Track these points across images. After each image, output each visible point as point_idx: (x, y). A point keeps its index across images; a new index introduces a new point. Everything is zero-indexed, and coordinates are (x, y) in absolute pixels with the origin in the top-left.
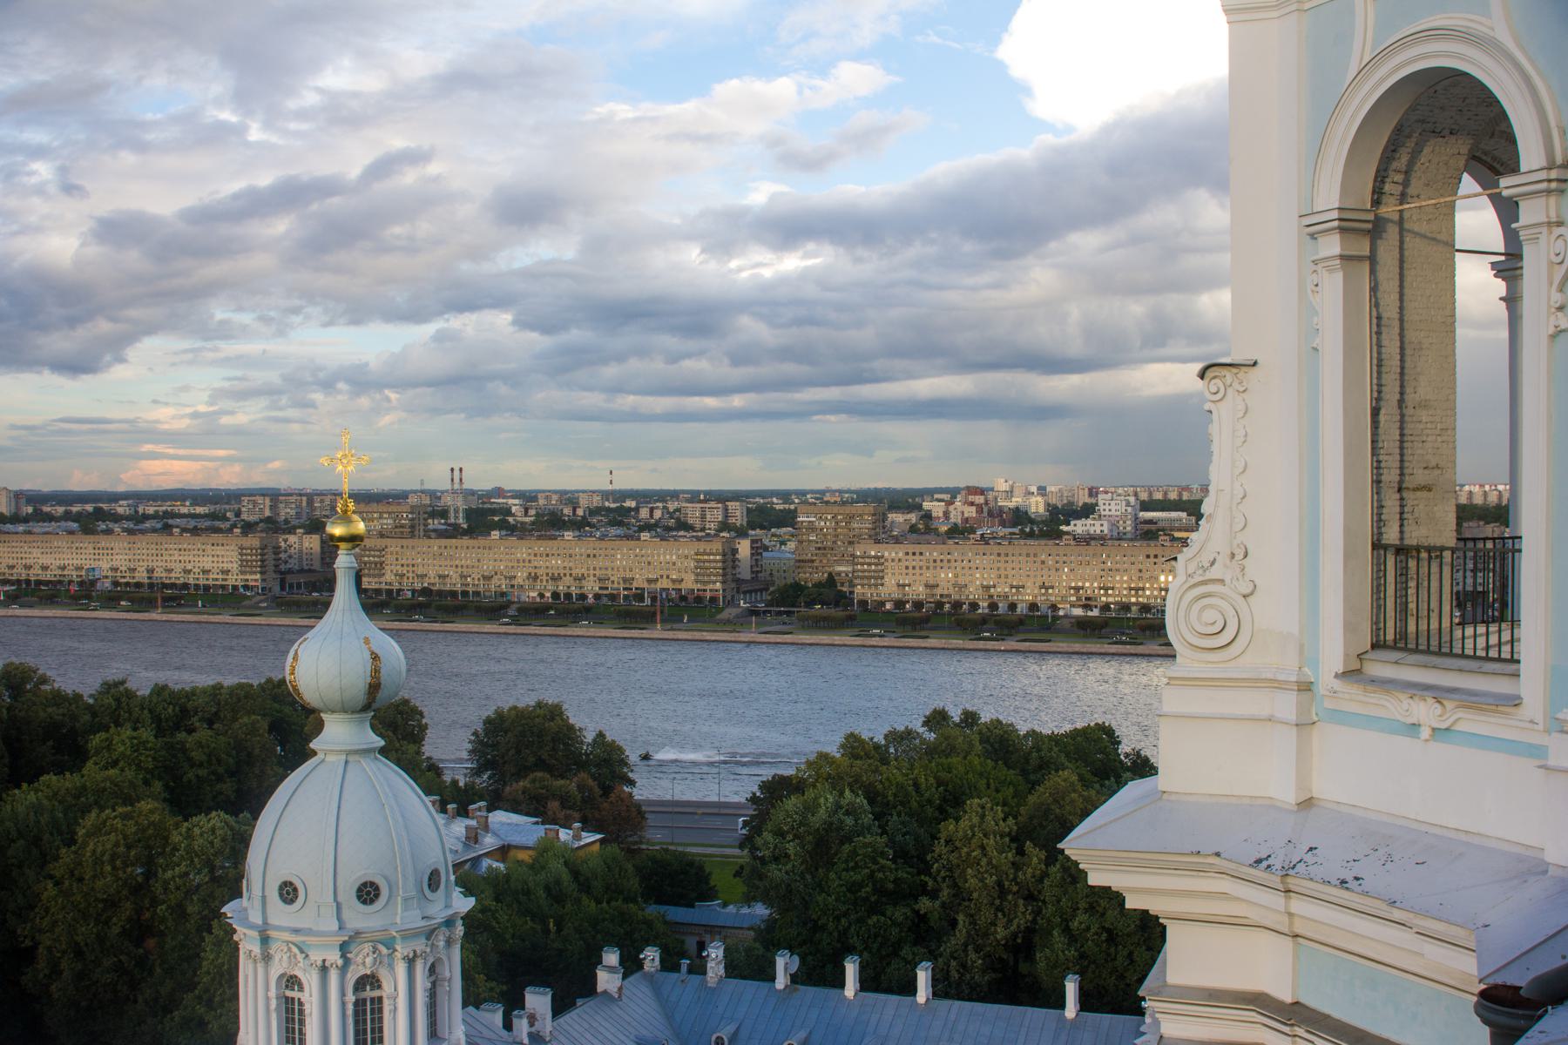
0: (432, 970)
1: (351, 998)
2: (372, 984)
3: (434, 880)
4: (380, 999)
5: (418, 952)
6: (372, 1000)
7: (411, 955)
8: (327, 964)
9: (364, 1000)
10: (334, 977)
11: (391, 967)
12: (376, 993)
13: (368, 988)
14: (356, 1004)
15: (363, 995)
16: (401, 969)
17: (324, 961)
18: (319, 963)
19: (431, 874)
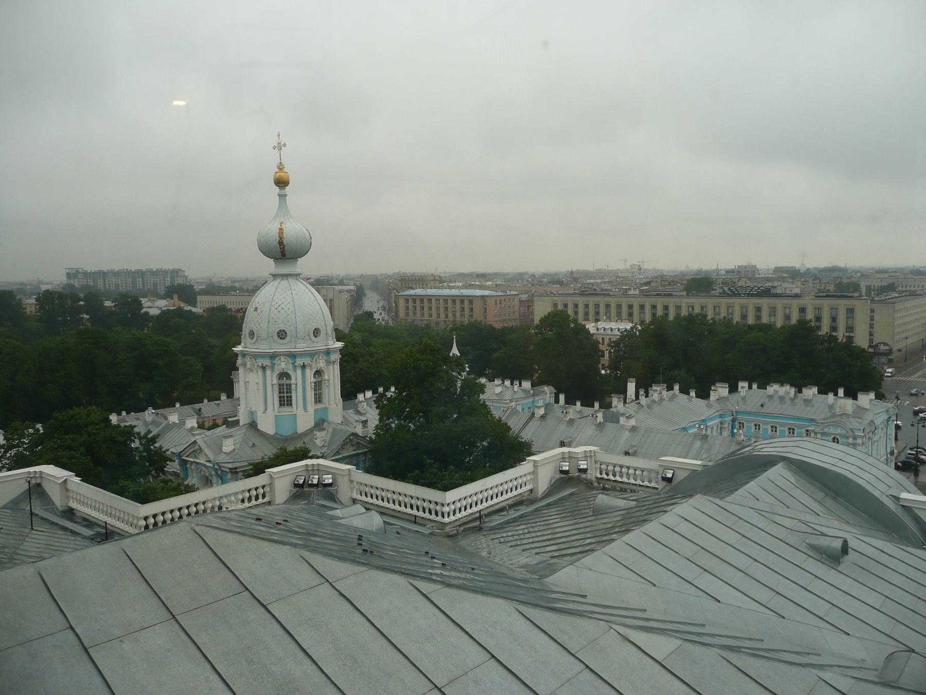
0: (318, 373)
1: (275, 381)
2: (286, 377)
3: (316, 332)
4: (290, 385)
5: (306, 364)
6: (287, 385)
7: (302, 364)
8: (264, 365)
9: (283, 385)
10: (268, 372)
11: (295, 370)
12: (288, 382)
13: (285, 378)
14: (280, 385)
15: (281, 382)
16: (299, 371)
17: (262, 364)
18: (260, 365)
19: (315, 329)
